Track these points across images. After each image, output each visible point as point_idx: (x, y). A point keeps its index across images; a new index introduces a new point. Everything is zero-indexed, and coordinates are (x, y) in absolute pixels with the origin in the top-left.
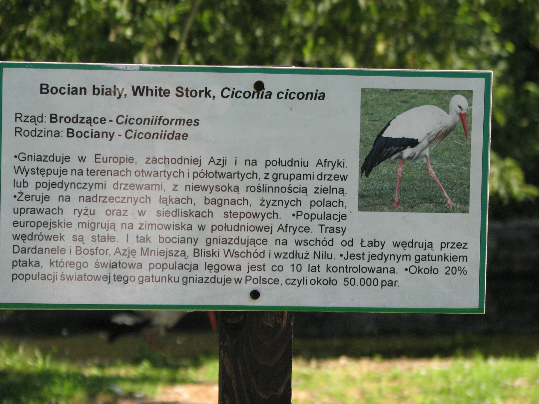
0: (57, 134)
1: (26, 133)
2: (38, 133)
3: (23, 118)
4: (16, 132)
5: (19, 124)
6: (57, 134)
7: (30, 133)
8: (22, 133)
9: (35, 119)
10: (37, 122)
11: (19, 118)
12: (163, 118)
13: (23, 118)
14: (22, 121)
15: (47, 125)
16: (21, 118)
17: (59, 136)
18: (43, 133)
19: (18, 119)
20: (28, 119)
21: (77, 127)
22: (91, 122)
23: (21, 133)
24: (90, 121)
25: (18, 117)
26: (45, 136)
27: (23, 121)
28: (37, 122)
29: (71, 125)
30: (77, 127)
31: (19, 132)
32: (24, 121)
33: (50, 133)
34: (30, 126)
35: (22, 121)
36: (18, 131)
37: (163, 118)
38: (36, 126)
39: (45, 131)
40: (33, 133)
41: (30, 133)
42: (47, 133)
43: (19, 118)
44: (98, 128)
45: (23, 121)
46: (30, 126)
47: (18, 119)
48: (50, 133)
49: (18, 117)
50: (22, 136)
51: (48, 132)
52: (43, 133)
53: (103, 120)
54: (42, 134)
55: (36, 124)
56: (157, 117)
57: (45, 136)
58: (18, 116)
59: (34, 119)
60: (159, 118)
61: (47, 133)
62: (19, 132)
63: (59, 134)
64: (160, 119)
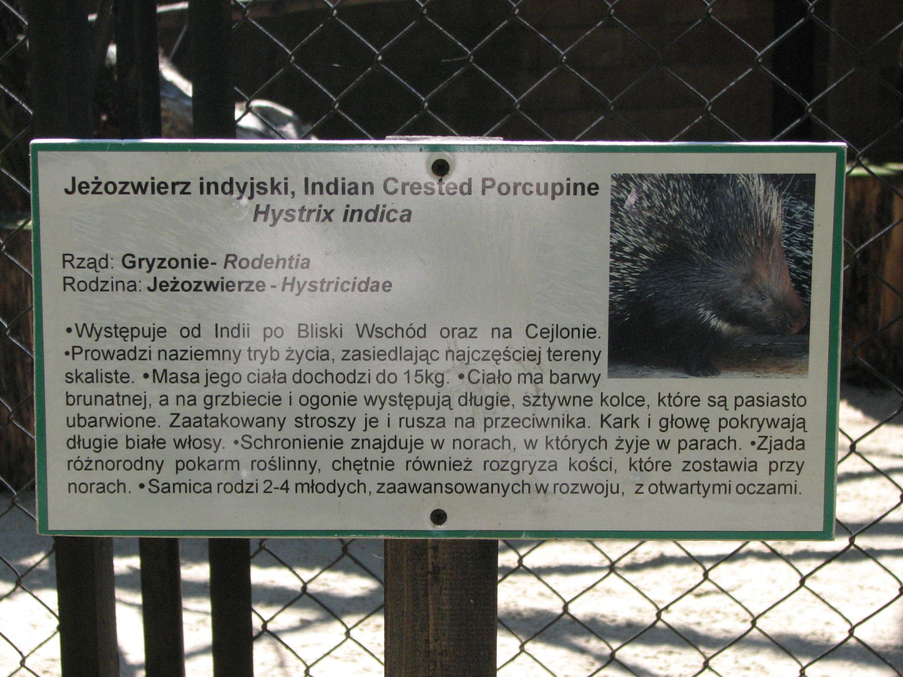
0: (133, 286)
1: (82, 286)
2: (101, 285)
3: (76, 262)
4: (65, 284)
5: (69, 271)
6: (133, 286)
7: (88, 286)
8: (75, 285)
9: (95, 263)
10: (98, 268)
11: (70, 261)
13: (76, 262)
14: (73, 267)
15: (117, 271)
17: (135, 289)
18: (110, 284)
19: (67, 264)
20: (85, 264)
23: (73, 285)
25: (67, 259)
26: (112, 290)
27: (76, 265)
28: (98, 268)
31: (70, 284)
32: (78, 267)
33: (120, 284)
34: (88, 275)
35: (73, 267)
36: (68, 283)
39: (112, 282)
40: (94, 286)
42: (115, 286)
43: (70, 261)
45: (76, 265)
46: (88, 275)
47: (67, 264)
48: (120, 284)
49: (67, 259)
50: (74, 290)
51: (117, 283)
52: (110, 284)
54: (108, 287)
55: (97, 270)
57: (112, 290)
58: (68, 258)
59: (93, 264)
61: (115, 286)
62: (70, 284)
63: (135, 286)
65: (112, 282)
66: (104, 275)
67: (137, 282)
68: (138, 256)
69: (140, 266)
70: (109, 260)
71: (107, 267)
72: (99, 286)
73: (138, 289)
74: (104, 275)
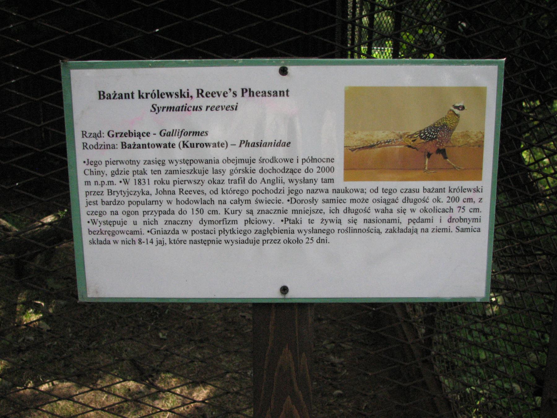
5: (85, 140)
6: (114, 147)
12: (184, 131)
21: (130, 140)
22: (140, 136)
24: (139, 135)
25: (84, 134)
29: (124, 139)
30: (130, 140)
35: (86, 137)
36: (85, 146)
37: (184, 131)
38: (97, 141)
44: (144, 140)
46: (92, 141)
49: (84, 134)
53: (148, 134)
56: (179, 130)
59: (96, 136)
60: (181, 131)
64: (182, 132)
66: (100, 141)
68: (115, 131)
69: (117, 136)
70: (102, 134)
71: (101, 137)
72: (97, 147)
73: (116, 147)
74: (100, 141)
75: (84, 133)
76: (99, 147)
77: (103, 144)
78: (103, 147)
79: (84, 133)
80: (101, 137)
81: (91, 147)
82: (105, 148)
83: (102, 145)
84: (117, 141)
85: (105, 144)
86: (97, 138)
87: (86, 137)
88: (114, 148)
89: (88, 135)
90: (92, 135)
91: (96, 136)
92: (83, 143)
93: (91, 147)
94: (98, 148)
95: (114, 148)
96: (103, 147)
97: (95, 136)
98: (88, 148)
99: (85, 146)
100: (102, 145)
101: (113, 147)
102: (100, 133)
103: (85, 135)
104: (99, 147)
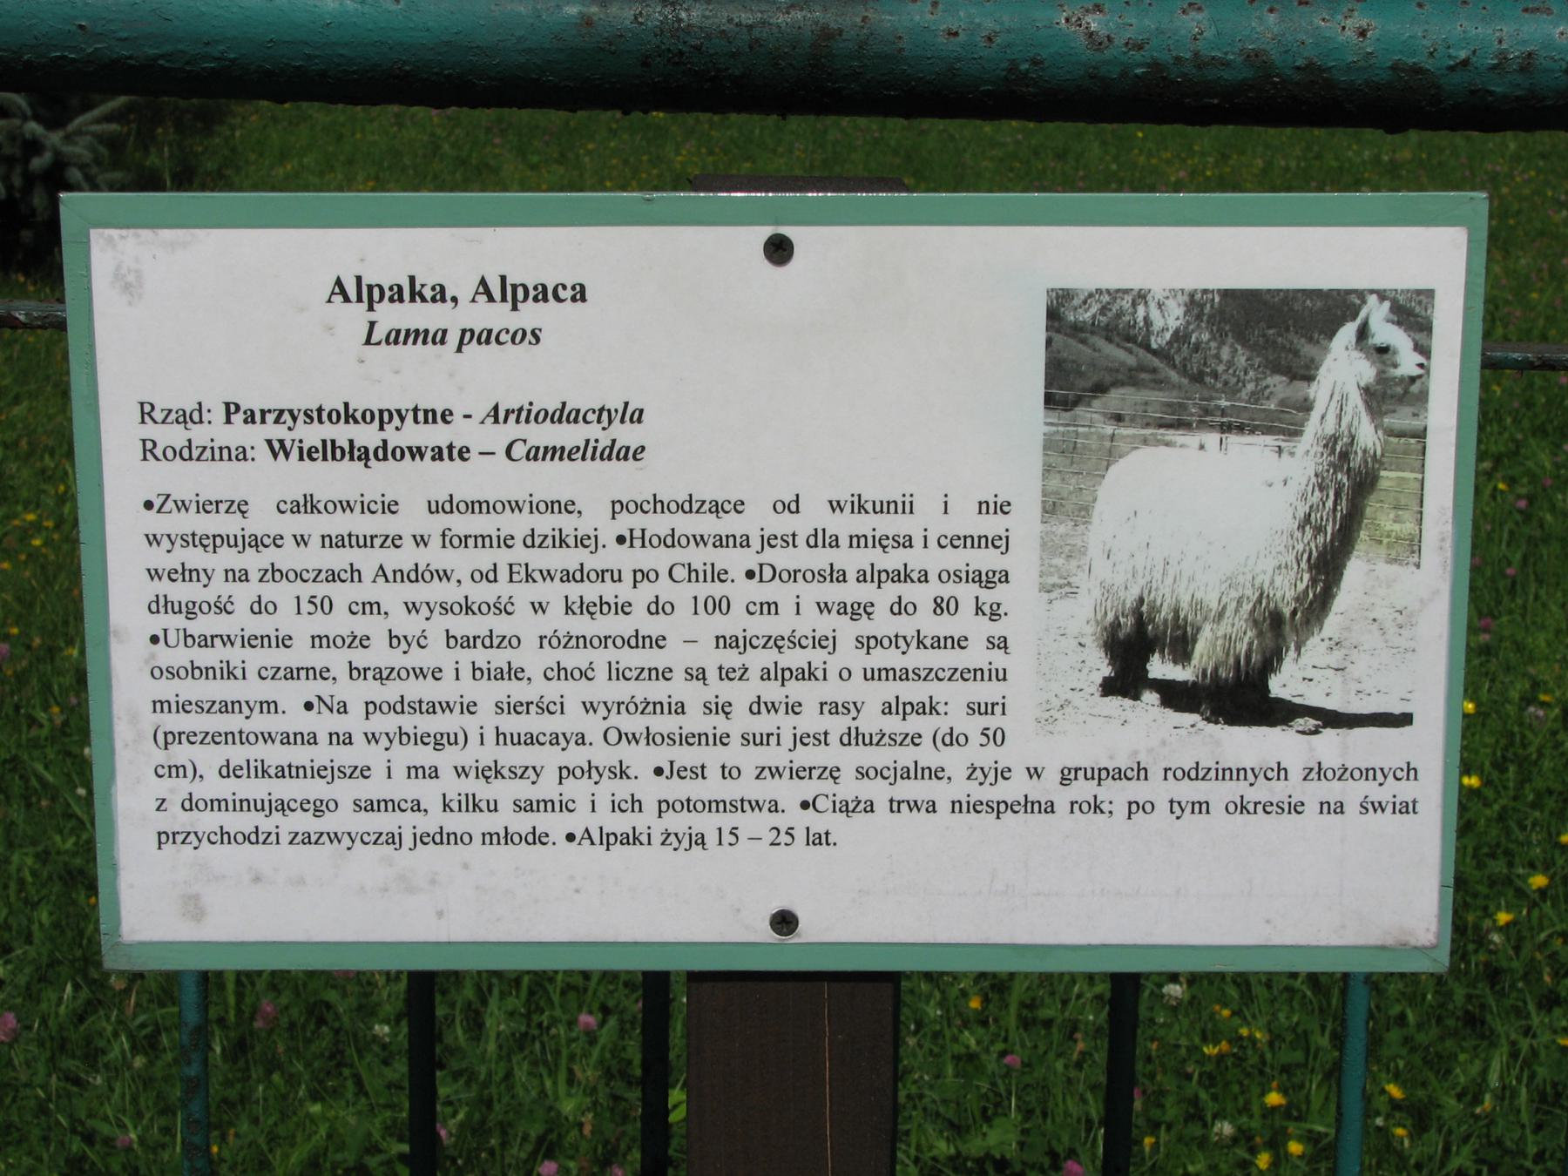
0: (243, 455)
5: (150, 431)
6: (243, 455)
16: (153, 414)
25: (146, 412)
34: (173, 436)
35: (155, 422)
36: (148, 450)
41: (178, 454)
46: (173, 436)
49: (146, 412)
59: (185, 419)
65: (212, 448)
66: (200, 435)
67: (249, 451)
71: (201, 422)
72: (187, 453)
73: (249, 456)
74: (200, 435)
75: (147, 408)
76: (195, 454)
77: (210, 444)
78: (208, 453)
79: (147, 408)
80: (201, 422)
81: (170, 453)
82: (213, 459)
83: (205, 448)
84: (255, 436)
85: (216, 445)
86: (190, 425)
87: (155, 422)
88: (245, 459)
89: (158, 416)
90: (173, 416)
91: (185, 419)
92: (144, 441)
93: (170, 453)
94: (191, 458)
95: (245, 459)
96: (208, 453)
97: (181, 419)
98: (160, 456)
99: (148, 450)
100: (205, 448)
101: (241, 456)
102: (200, 411)
103: (149, 414)
104: (195, 454)
